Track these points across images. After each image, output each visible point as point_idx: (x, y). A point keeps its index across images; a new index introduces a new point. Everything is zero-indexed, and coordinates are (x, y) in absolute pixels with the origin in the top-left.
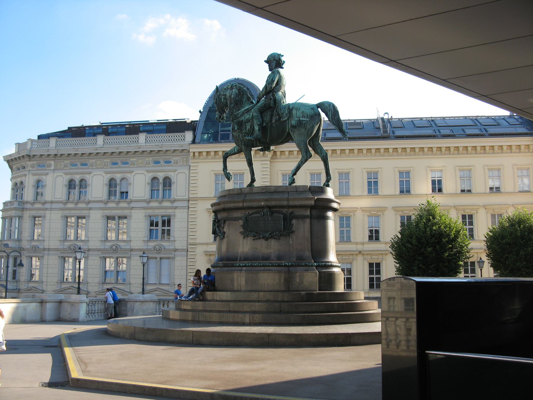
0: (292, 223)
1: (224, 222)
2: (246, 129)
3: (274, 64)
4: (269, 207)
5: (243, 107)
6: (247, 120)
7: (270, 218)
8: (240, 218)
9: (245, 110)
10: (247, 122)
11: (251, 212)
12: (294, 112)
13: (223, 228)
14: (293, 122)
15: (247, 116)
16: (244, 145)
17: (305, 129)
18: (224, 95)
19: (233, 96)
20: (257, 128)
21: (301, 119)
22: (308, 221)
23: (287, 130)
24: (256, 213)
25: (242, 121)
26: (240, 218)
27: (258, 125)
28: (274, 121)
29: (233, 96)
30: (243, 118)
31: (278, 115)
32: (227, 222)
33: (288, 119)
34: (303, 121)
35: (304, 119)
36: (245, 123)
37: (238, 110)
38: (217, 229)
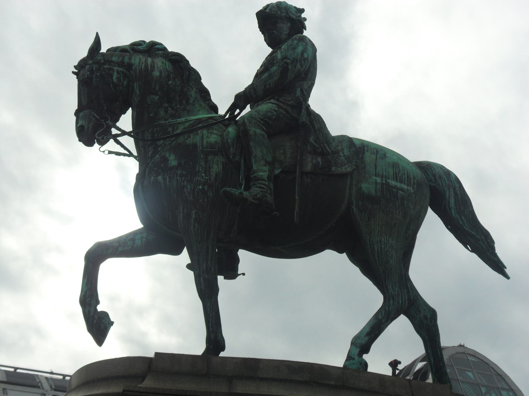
3: (285, 27)
5: (190, 113)
6: (211, 146)
9: (200, 121)
12: (368, 157)
14: (367, 187)
15: (213, 138)
18: (121, 64)
19: (156, 73)
20: (262, 171)
21: (393, 183)
25: (195, 146)
27: (267, 163)
29: (156, 73)
30: (195, 139)
34: (395, 187)
35: (399, 185)
37: (173, 116)
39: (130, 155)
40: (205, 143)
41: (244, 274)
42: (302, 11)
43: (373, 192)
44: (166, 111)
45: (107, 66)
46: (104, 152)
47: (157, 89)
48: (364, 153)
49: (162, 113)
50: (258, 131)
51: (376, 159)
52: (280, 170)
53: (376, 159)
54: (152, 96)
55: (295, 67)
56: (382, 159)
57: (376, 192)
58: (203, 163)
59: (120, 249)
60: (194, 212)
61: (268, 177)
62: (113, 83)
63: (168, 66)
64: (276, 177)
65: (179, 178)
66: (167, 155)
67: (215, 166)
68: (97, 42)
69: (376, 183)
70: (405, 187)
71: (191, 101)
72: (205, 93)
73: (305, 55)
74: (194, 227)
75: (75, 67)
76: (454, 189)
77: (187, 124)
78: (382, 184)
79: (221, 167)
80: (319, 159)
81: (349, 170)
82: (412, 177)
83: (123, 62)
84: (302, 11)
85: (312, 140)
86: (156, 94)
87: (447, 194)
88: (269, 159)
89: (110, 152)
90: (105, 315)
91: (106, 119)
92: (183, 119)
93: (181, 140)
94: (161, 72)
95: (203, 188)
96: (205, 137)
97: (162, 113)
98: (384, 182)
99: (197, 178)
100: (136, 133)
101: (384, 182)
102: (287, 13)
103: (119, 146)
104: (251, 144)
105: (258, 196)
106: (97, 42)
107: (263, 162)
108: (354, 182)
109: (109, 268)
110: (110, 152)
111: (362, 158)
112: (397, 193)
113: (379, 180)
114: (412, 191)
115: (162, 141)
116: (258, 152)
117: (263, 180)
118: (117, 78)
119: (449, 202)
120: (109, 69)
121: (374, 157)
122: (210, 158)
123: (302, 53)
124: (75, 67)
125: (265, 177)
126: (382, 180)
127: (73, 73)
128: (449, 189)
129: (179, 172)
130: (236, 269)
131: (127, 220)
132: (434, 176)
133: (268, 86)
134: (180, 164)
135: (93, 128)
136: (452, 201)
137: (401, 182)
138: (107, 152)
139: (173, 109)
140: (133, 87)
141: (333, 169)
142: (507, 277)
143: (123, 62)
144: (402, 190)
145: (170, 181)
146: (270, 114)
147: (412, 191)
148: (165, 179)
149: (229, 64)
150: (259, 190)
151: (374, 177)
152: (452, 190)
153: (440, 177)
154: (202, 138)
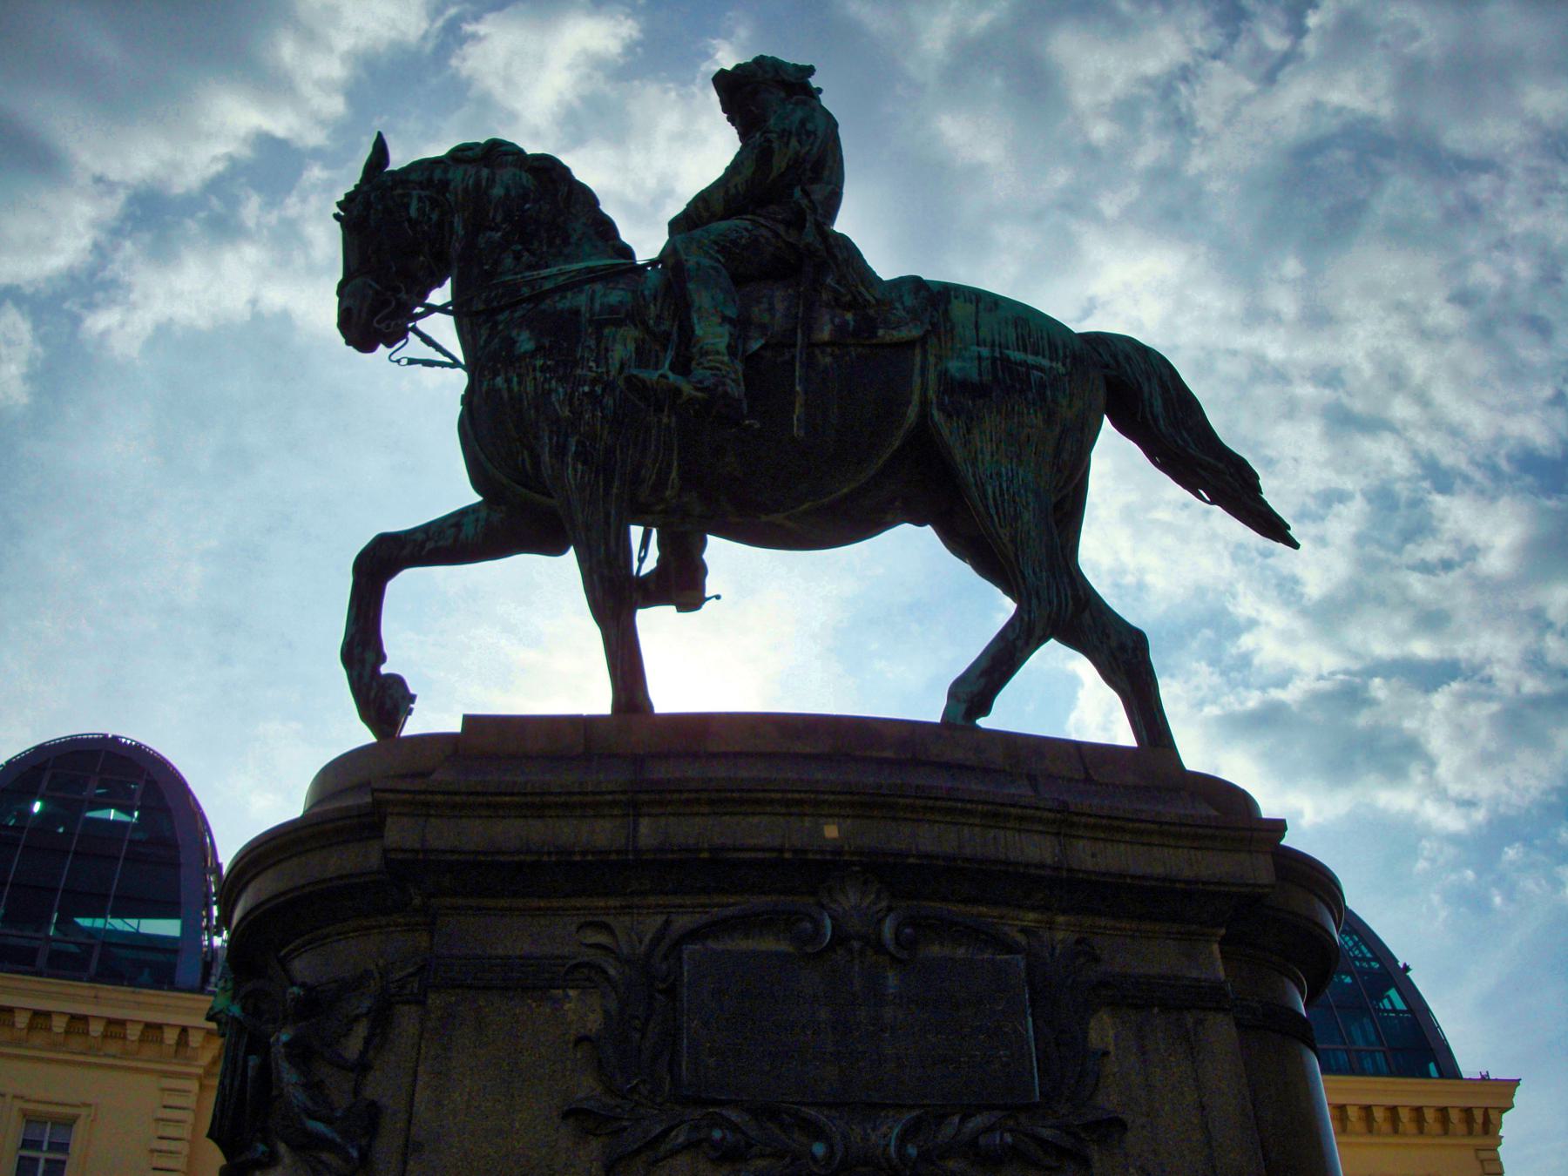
0: (1094, 1039)
1: (381, 1019)
2: (602, 356)
4: (885, 871)
6: (613, 309)
7: (892, 980)
8: (583, 974)
10: (618, 323)
11: (682, 922)
12: (959, 310)
13: (362, 1067)
15: (614, 297)
16: (583, 456)
17: (1050, 418)
20: (712, 334)
22: (1221, 1032)
23: (912, 413)
24: (745, 923)
26: (583, 974)
28: (825, 333)
31: (855, 304)
32: (407, 1021)
33: (923, 340)
34: (1024, 363)
35: (1031, 359)
36: (599, 325)
38: (289, 1076)
39: (455, 364)
40: (597, 306)
41: (718, 597)
42: (810, 70)
43: (975, 377)
44: (517, 257)
45: (399, 191)
46: (398, 361)
47: (499, 219)
48: (948, 302)
49: (508, 261)
50: (706, 262)
51: (977, 312)
52: (761, 342)
53: (977, 312)
54: (488, 234)
55: (787, 144)
56: (990, 310)
57: (980, 375)
58: (592, 343)
59: (429, 545)
60: (573, 441)
61: (729, 346)
62: (410, 220)
63: (527, 179)
64: (751, 360)
65: (538, 374)
66: (514, 333)
67: (619, 347)
68: (380, 151)
69: (980, 358)
70: (1046, 363)
71: (574, 238)
72: (606, 228)
73: (809, 126)
74: (575, 470)
75: (339, 204)
76: (1160, 378)
77: (562, 278)
78: (994, 360)
79: (631, 346)
80: (849, 316)
81: (916, 333)
82: (1060, 343)
83: (430, 180)
84: (810, 70)
85: (829, 281)
86: (496, 229)
87: (1146, 389)
88: (731, 312)
89: (412, 362)
90: (397, 681)
91: (396, 290)
92: (554, 270)
93: (546, 305)
94: (507, 189)
95: (592, 391)
96: (598, 295)
97: (508, 261)
98: (997, 354)
99: (579, 371)
100: (458, 309)
101: (997, 354)
102: (777, 71)
103: (431, 349)
104: (691, 286)
105: (706, 384)
106: (380, 151)
107: (716, 319)
108: (932, 359)
109: (407, 589)
110: (412, 362)
111: (946, 311)
112: (1028, 375)
113: (985, 352)
114: (1062, 370)
115: (507, 314)
116: (702, 299)
117: (718, 353)
118: (418, 210)
119: (1151, 406)
120: (403, 196)
121: (971, 308)
122: (606, 331)
123: (803, 123)
124: (339, 204)
125: (722, 347)
126: (993, 351)
127: (337, 217)
128: (1149, 379)
129: (539, 363)
130: (700, 587)
131: (451, 489)
132: (1114, 357)
133: (732, 191)
134: (539, 348)
135: (372, 317)
136: (1158, 403)
137: (1036, 353)
138: (404, 362)
139: (533, 254)
140: (452, 223)
141: (881, 332)
142: (1295, 546)
143: (430, 180)
144: (1040, 368)
145: (519, 383)
146: (735, 235)
147: (1062, 370)
148: (508, 381)
149: (656, 169)
150: (708, 373)
151: (974, 348)
152: (1155, 381)
153: (1128, 357)
154: (592, 299)
